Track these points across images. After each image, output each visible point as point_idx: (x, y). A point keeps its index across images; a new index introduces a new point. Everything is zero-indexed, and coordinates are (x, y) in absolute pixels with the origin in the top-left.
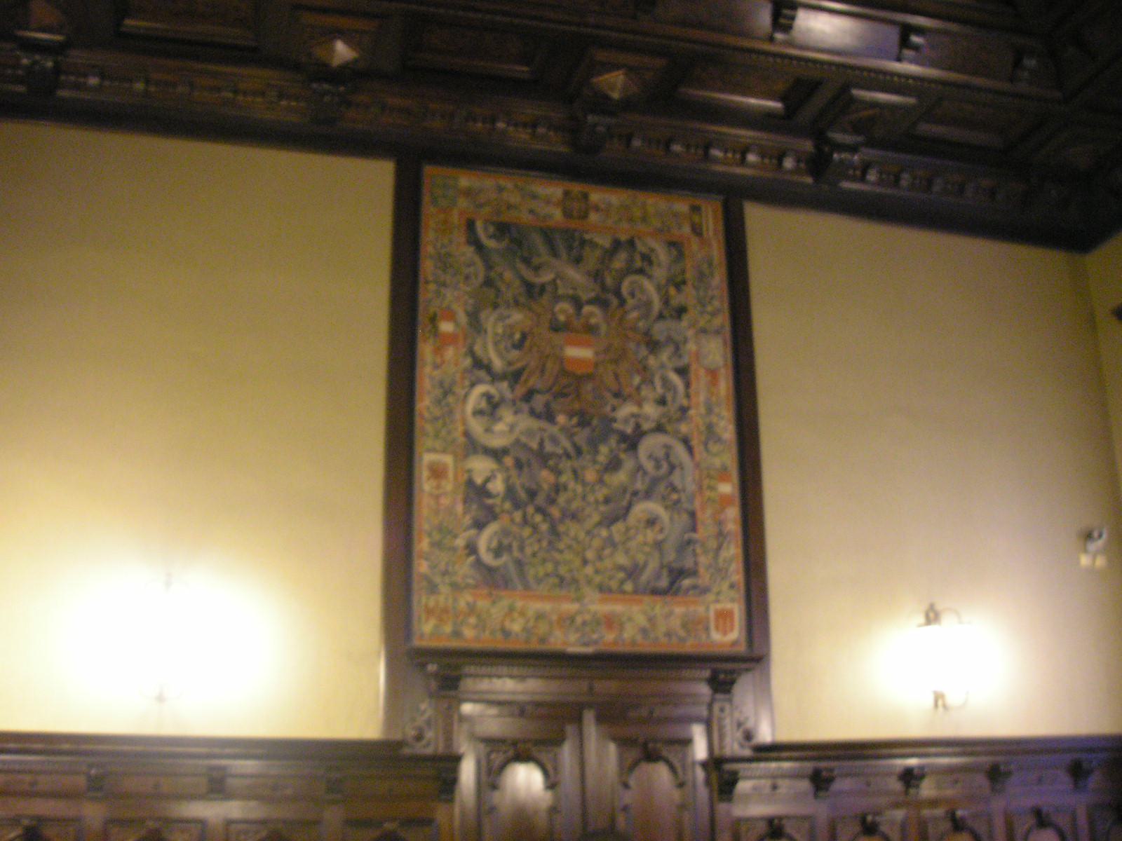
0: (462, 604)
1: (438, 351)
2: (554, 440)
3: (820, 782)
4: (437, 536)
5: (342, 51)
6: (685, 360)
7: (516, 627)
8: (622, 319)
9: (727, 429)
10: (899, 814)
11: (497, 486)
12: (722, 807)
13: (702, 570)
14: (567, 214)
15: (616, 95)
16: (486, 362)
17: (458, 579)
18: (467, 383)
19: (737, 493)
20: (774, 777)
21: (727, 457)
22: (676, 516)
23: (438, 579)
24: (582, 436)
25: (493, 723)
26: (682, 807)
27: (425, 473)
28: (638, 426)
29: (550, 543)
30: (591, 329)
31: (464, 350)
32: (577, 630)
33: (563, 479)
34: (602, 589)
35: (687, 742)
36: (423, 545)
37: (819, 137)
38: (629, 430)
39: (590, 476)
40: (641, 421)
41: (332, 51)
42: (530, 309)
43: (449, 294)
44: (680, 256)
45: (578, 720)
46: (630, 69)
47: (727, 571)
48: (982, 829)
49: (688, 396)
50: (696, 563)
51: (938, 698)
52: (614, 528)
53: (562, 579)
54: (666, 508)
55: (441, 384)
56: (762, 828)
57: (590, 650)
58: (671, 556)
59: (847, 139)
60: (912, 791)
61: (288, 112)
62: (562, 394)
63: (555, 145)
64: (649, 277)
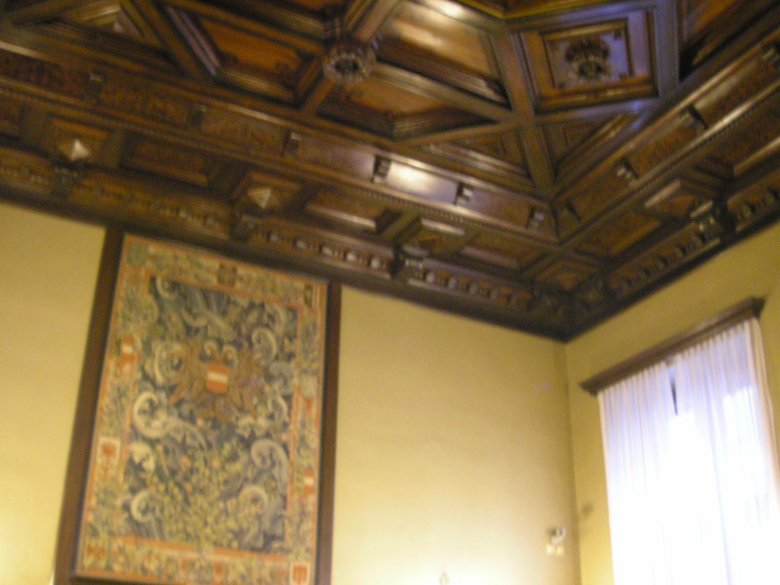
0: (115, 547)
1: (119, 365)
2: (193, 436)
4: (102, 496)
5: (79, 150)
7: (152, 566)
8: (249, 358)
9: (314, 440)
11: (150, 465)
13: (288, 537)
14: (221, 280)
15: (263, 205)
16: (151, 375)
17: (115, 529)
18: (137, 390)
19: (316, 486)
21: (312, 460)
22: (273, 498)
23: (99, 527)
24: (213, 436)
28: (253, 433)
29: (183, 510)
30: (227, 362)
34: (217, 544)
36: (91, 501)
37: (398, 248)
38: (246, 434)
39: (216, 464)
42: (188, 344)
43: (132, 327)
46: (276, 189)
49: (289, 414)
50: (284, 533)
52: (229, 503)
54: (267, 492)
58: (267, 525)
61: (35, 185)
62: (203, 405)
63: (220, 233)
64: (272, 331)
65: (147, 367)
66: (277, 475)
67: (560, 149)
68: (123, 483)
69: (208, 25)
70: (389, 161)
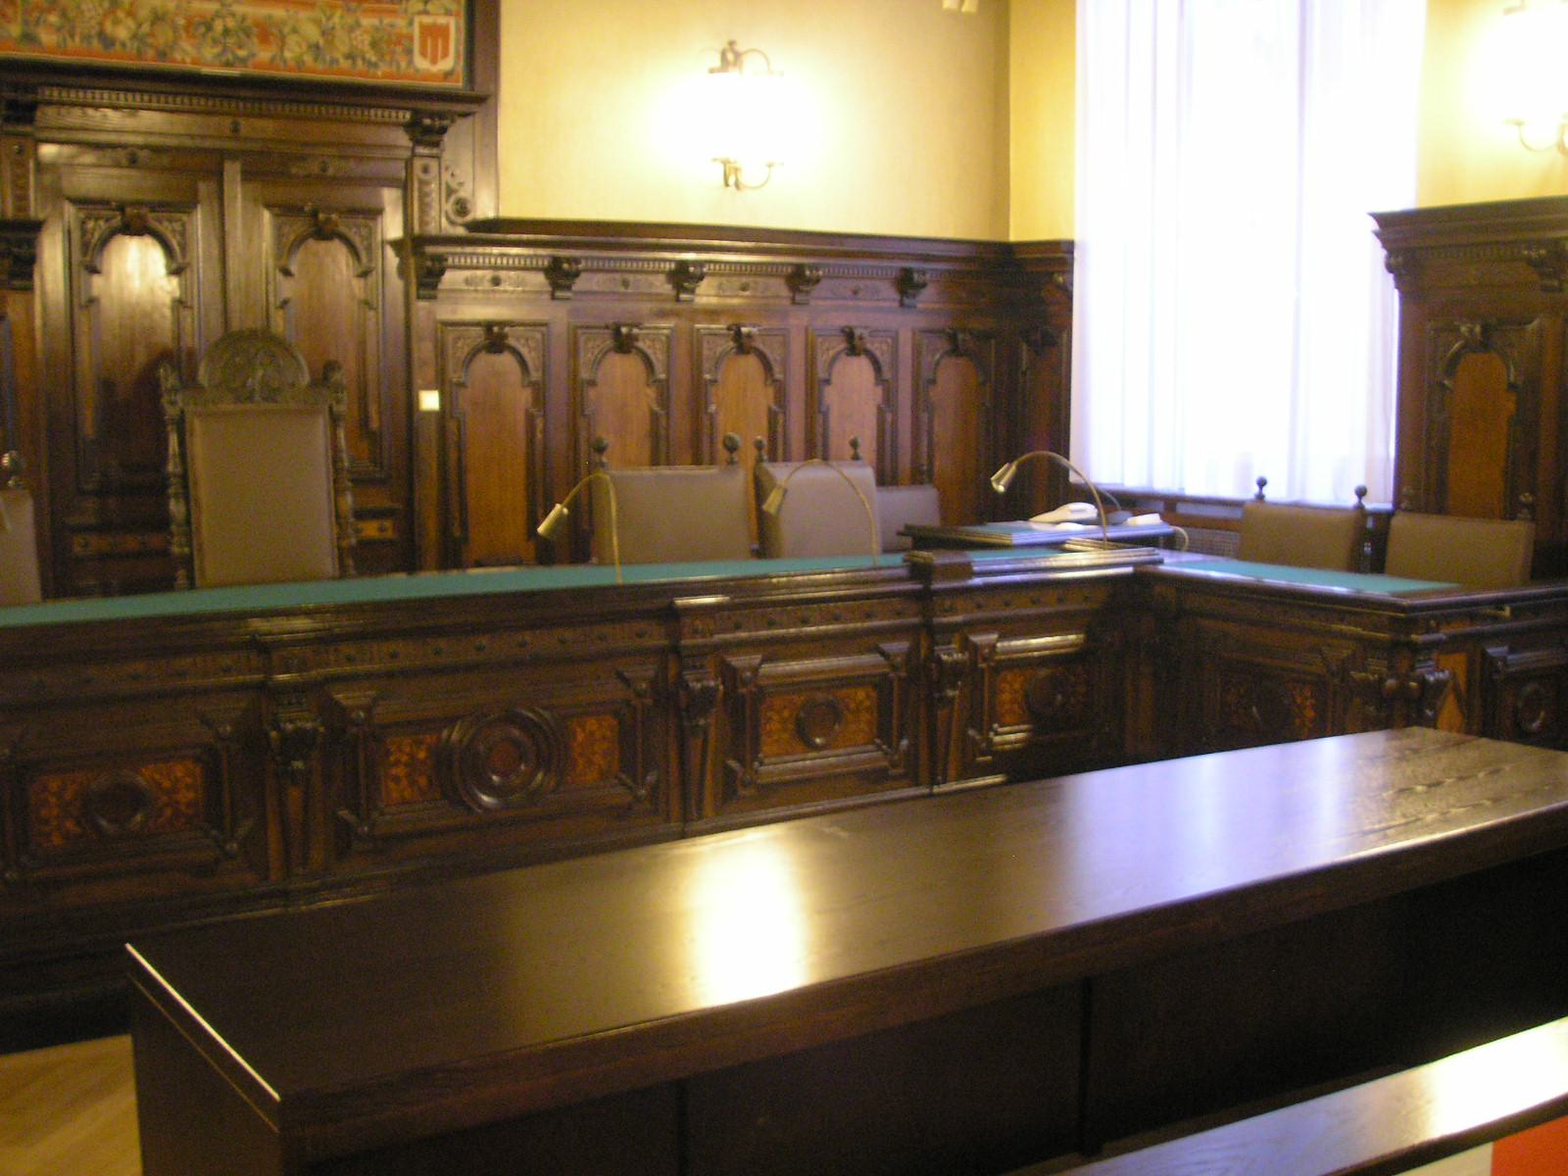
3: (559, 276)
7: (122, 33)
12: (421, 306)
20: (495, 268)
25: (95, 178)
26: (367, 304)
32: (215, 42)
35: (376, 213)
45: (218, 175)
48: (774, 356)
56: (477, 335)
60: (683, 296)
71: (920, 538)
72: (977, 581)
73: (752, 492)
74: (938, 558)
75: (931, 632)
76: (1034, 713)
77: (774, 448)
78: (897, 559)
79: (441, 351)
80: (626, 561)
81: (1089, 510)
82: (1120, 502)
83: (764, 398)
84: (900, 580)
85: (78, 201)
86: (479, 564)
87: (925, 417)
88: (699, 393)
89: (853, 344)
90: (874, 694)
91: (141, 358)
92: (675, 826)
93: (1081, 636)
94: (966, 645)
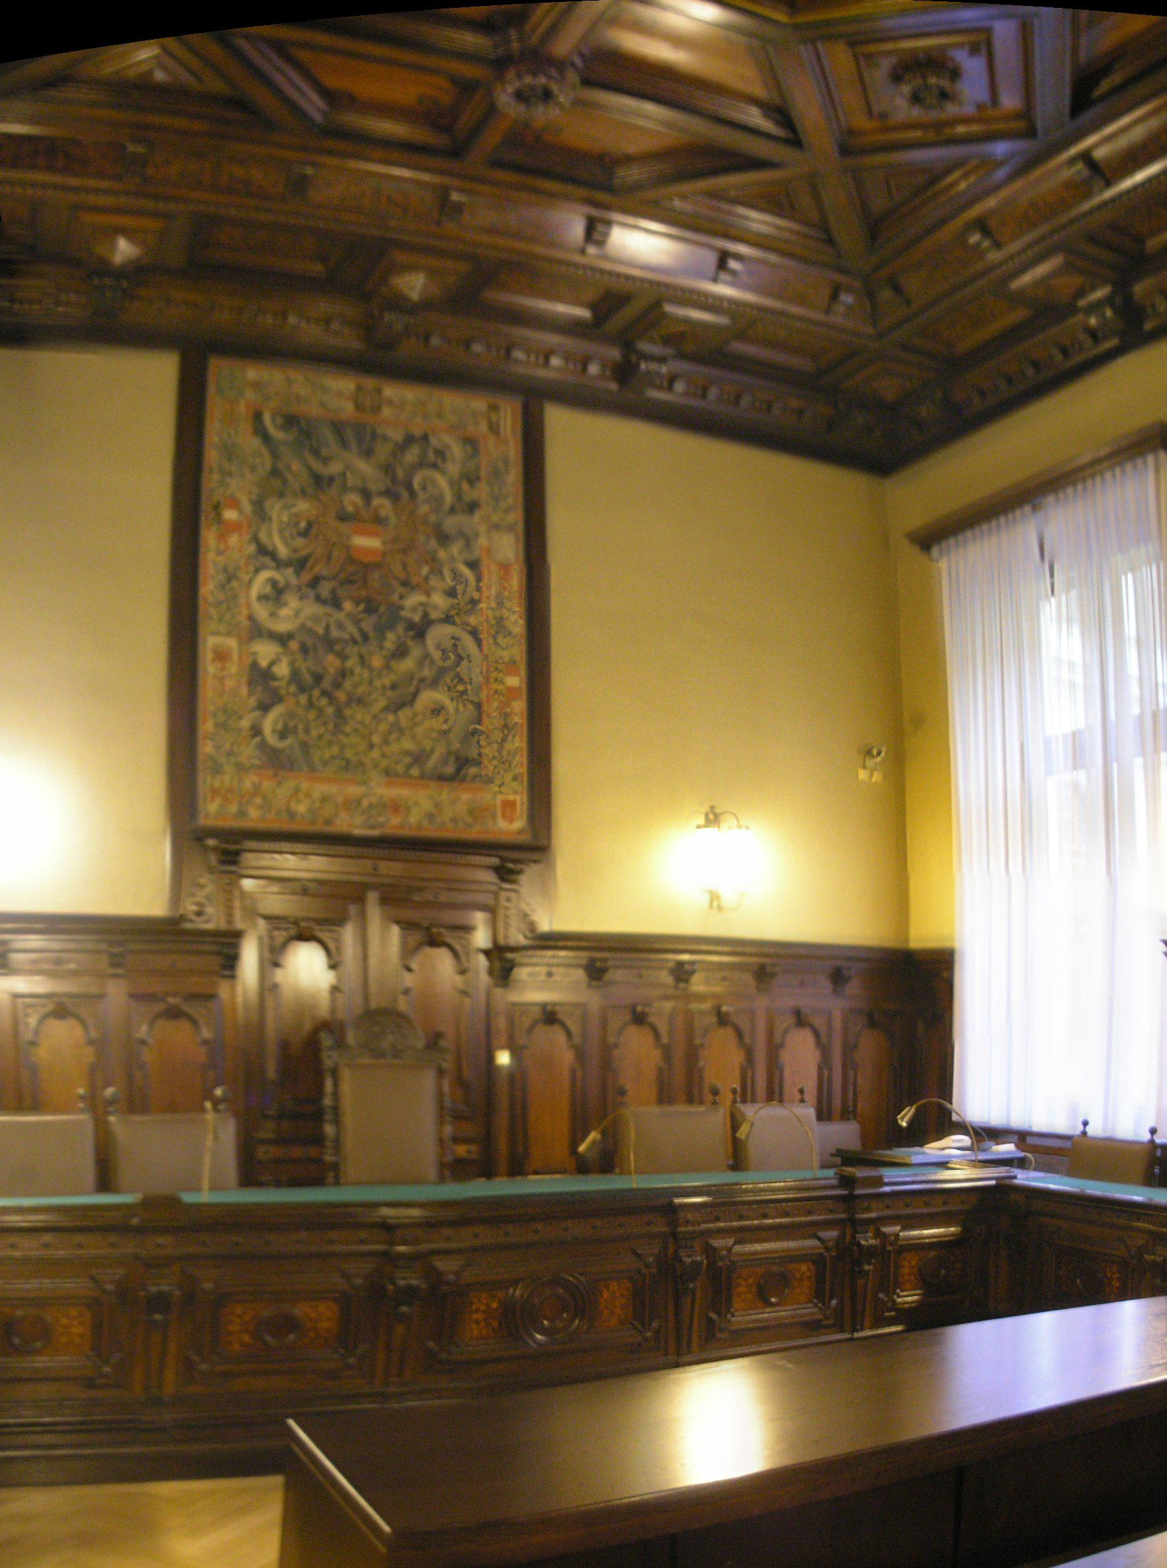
0: (247, 784)
1: (221, 537)
2: (340, 626)
3: (596, 973)
5: (124, 250)
6: (476, 553)
9: (517, 623)
10: (668, 1006)
11: (282, 669)
12: (498, 991)
13: (486, 761)
14: (359, 407)
15: (415, 296)
16: (270, 548)
17: (243, 759)
18: (251, 568)
19: (524, 687)
20: (549, 965)
21: (515, 650)
23: (222, 760)
24: (368, 624)
27: (210, 656)
28: (426, 615)
29: (336, 725)
30: (379, 520)
31: (248, 537)
33: (350, 663)
34: (387, 773)
35: (468, 929)
36: (206, 726)
37: (626, 342)
38: (417, 618)
39: (377, 662)
40: (429, 610)
41: (113, 247)
42: (320, 501)
43: (234, 483)
44: (476, 452)
45: (361, 900)
46: (431, 272)
47: (511, 762)
48: (745, 1026)
49: (479, 589)
50: (480, 755)
51: (714, 897)
52: (401, 714)
53: (348, 762)
55: (225, 569)
56: (536, 1013)
57: (376, 833)
59: (657, 350)
60: (681, 985)
63: (348, 340)
64: (443, 472)
65: (262, 536)
66: (465, 676)
67: (879, 204)
68: (247, 699)
69: (303, 55)
70: (609, 223)
71: (847, 1158)
72: (887, 1189)
73: (729, 1124)
74: (860, 1172)
75: (855, 1225)
76: (926, 1282)
77: (745, 1093)
78: (830, 1173)
79: (511, 1021)
80: (639, 1172)
81: (965, 1140)
82: (986, 1134)
83: (736, 1057)
84: (832, 1187)
85: (267, 918)
86: (536, 1173)
87: (851, 1073)
88: (692, 1054)
89: (800, 1019)
90: (813, 1268)
91: (308, 1026)
92: (671, 1358)
93: (959, 1228)
94: (878, 1234)
